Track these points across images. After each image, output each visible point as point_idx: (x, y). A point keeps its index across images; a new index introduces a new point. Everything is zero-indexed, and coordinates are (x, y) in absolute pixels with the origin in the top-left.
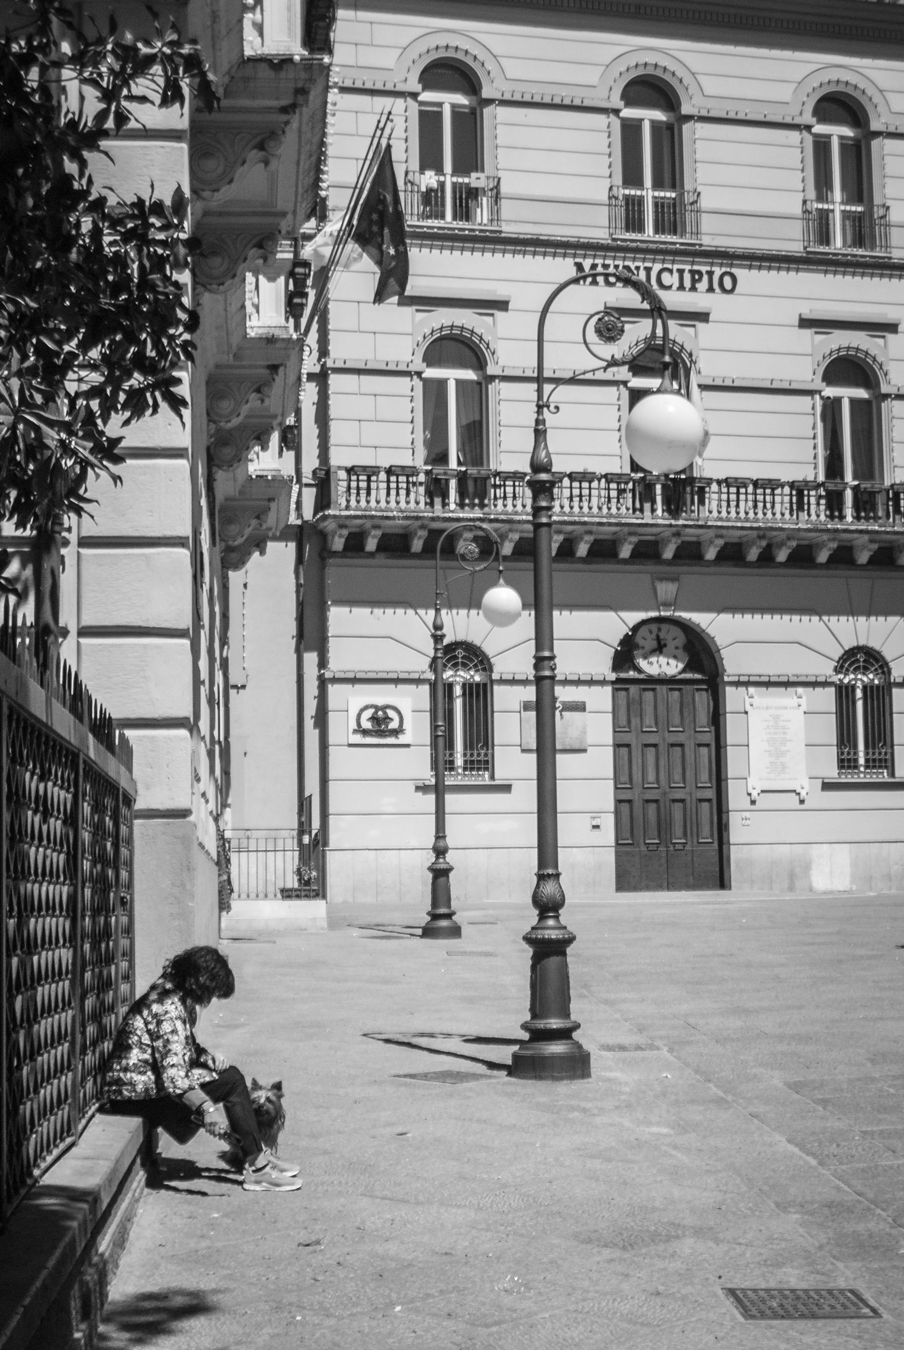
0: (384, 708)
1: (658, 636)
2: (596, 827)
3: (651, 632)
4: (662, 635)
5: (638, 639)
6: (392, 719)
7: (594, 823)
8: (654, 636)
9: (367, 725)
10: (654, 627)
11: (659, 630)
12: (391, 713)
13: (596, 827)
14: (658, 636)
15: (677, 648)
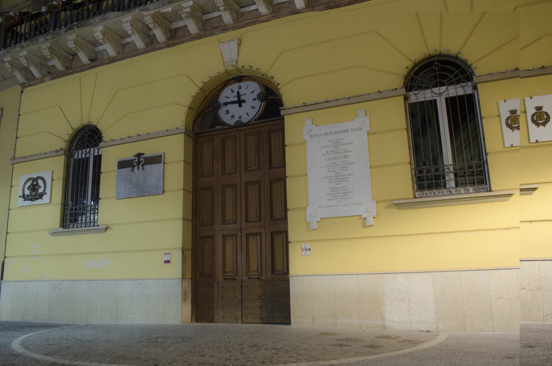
0: (35, 180)
1: (238, 93)
2: (167, 262)
3: (233, 91)
4: (242, 92)
5: (222, 99)
6: (40, 187)
7: (166, 259)
8: (235, 94)
9: (27, 192)
10: (235, 87)
11: (240, 88)
12: (41, 182)
13: (167, 262)
14: (238, 93)
15: (254, 99)
